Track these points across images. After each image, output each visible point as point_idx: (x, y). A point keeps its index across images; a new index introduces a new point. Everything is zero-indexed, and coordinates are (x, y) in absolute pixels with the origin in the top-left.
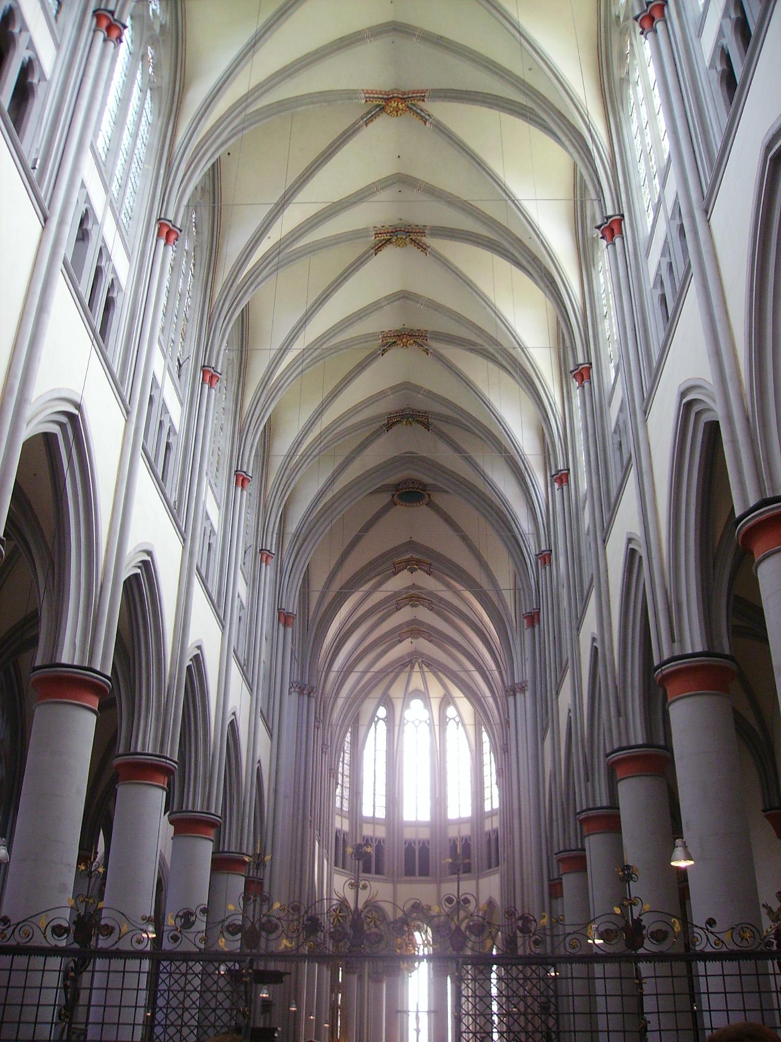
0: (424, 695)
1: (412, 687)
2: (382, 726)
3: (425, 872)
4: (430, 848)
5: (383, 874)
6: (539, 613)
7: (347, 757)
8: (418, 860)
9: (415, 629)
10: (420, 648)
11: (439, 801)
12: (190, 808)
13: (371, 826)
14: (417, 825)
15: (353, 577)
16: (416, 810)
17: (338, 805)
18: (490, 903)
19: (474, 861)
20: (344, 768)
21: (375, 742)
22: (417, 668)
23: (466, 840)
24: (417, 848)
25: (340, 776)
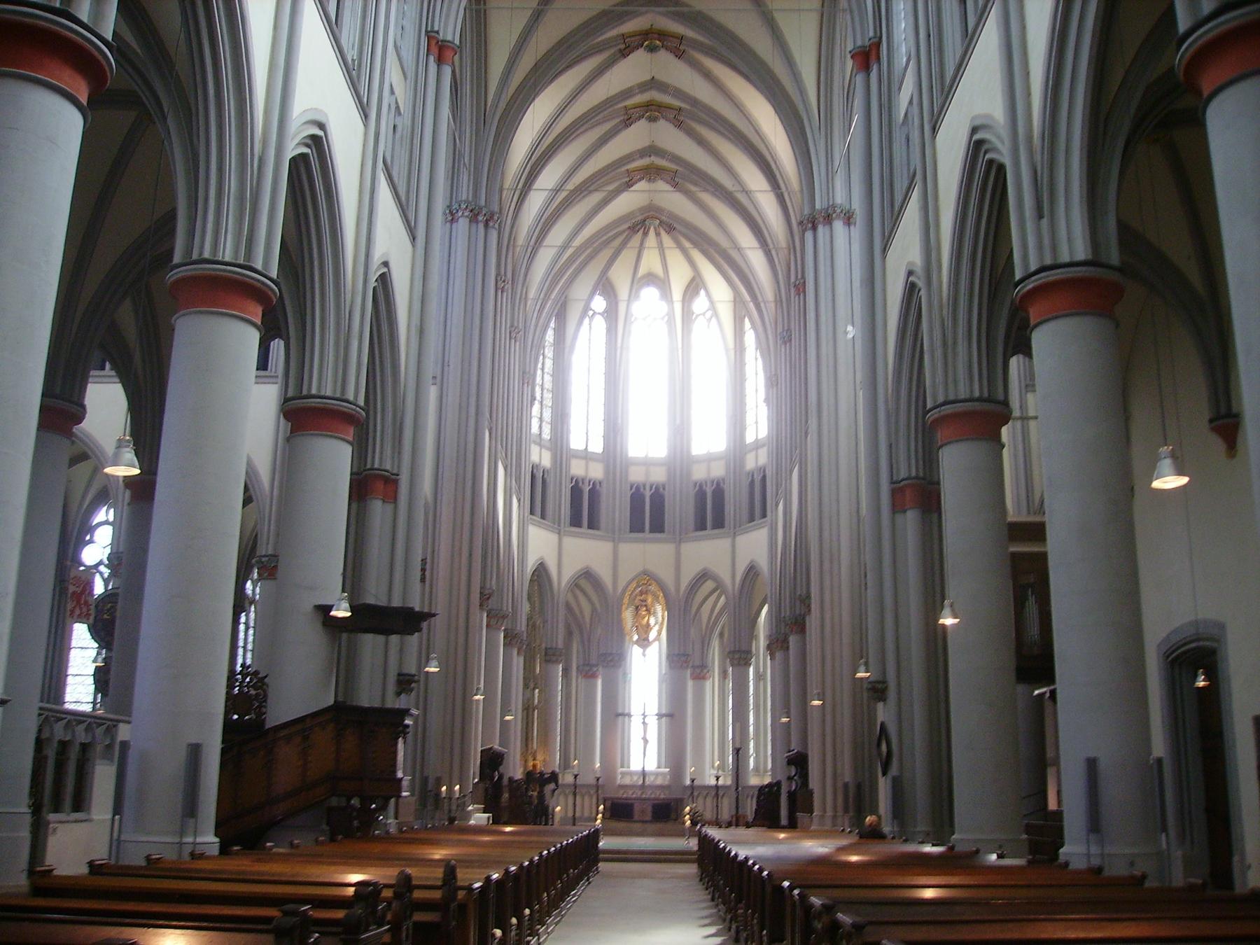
0: (663, 284)
1: (642, 271)
2: (600, 324)
3: (658, 526)
4: (666, 493)
5: (598, 529)
6: (878, 45)
7: (549, 364)
8: (648, 512)
9: (655, 164)
10: (660, 196)
11: (680, 431)
12: (206, 255)
13: (583, 462)
14: (647, 463)
15: (560, 43)
16: (647, 444)
17: (535, 429)
18: (752, 571)
19: (729, 509)
20: (544, 378)
21: (588, 341)
22: (651, 239)
23: (718, 484)
24: (648, 494)
25: (538, 389)
